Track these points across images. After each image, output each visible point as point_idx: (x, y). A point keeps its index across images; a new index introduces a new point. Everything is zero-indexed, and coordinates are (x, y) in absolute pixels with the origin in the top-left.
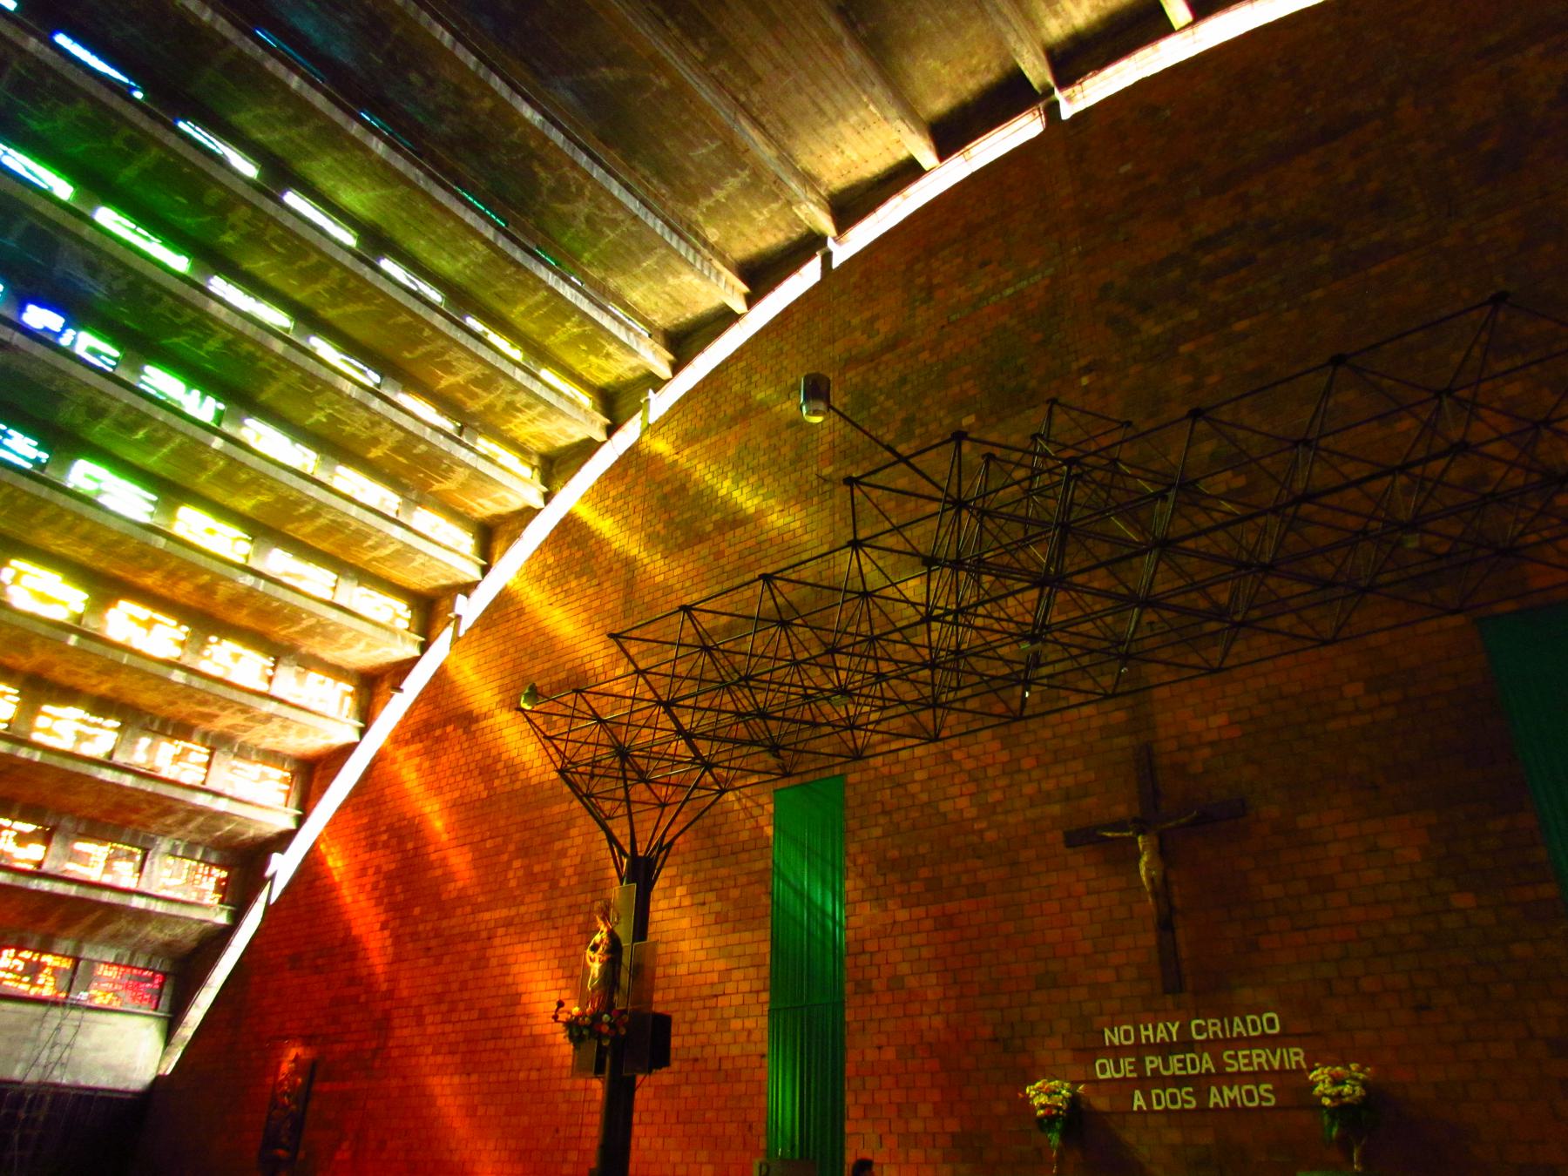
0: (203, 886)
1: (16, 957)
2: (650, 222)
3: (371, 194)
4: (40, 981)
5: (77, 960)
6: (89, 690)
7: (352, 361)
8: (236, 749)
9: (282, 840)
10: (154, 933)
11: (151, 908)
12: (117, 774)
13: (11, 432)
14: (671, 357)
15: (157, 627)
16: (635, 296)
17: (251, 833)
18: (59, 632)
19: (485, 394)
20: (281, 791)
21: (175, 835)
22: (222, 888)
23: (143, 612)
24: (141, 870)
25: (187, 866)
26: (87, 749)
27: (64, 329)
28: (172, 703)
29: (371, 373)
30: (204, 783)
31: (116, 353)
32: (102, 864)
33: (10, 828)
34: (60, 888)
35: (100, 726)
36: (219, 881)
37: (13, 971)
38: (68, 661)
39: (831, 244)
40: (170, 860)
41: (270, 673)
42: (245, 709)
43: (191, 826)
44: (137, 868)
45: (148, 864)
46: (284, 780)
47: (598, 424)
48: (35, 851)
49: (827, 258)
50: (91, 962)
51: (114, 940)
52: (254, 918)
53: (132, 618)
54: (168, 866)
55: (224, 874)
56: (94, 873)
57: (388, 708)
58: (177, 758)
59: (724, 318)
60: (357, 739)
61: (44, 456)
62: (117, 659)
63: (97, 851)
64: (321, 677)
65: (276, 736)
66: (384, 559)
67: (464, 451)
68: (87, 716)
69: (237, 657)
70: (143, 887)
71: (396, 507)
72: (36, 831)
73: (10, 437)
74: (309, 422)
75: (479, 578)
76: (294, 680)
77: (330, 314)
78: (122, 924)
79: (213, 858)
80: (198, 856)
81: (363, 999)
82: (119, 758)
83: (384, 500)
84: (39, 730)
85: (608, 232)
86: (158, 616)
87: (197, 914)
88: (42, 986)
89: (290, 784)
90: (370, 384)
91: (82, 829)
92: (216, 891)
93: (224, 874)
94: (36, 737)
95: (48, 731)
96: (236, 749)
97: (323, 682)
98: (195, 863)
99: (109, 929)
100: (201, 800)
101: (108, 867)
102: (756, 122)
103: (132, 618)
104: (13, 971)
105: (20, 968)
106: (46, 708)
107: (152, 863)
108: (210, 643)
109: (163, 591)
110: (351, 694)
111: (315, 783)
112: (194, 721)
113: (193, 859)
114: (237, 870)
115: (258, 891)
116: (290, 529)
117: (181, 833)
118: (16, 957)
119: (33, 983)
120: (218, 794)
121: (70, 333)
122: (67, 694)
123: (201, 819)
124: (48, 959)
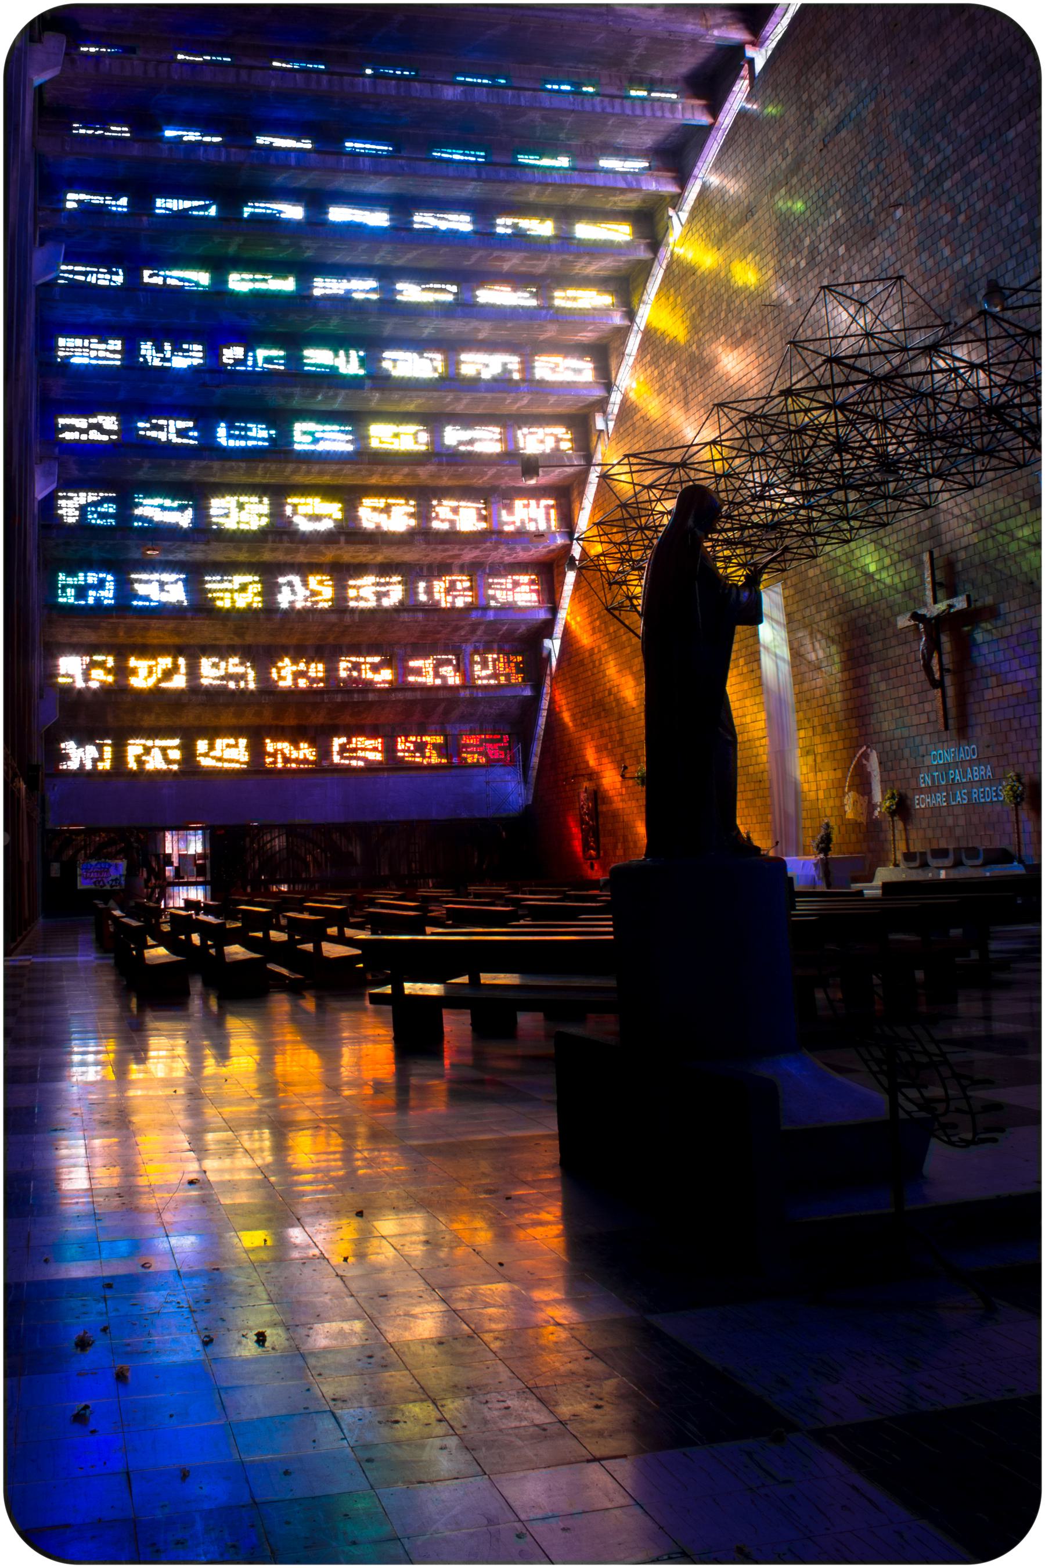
6: (373, 562)
7: (431, 286)
13: (249, 425)
27: (246, 355)
29: (449, 287)
31: (282, 353)
33: (365, 663)
35: (388, 584)
59: (704, 133)
60: (568, 542)
61: (273, 432)
68: (378, 579)
73: (250, 429)
74: (424, 335)
77: (399, 263)
82: (407, 602)
83: (505, 365)
84: (352, 599)
91: (409, 650)
94: (352, 604)
95: (358, 598)
106: (351, 582)
121: (250, 354)
122: (360, 569)
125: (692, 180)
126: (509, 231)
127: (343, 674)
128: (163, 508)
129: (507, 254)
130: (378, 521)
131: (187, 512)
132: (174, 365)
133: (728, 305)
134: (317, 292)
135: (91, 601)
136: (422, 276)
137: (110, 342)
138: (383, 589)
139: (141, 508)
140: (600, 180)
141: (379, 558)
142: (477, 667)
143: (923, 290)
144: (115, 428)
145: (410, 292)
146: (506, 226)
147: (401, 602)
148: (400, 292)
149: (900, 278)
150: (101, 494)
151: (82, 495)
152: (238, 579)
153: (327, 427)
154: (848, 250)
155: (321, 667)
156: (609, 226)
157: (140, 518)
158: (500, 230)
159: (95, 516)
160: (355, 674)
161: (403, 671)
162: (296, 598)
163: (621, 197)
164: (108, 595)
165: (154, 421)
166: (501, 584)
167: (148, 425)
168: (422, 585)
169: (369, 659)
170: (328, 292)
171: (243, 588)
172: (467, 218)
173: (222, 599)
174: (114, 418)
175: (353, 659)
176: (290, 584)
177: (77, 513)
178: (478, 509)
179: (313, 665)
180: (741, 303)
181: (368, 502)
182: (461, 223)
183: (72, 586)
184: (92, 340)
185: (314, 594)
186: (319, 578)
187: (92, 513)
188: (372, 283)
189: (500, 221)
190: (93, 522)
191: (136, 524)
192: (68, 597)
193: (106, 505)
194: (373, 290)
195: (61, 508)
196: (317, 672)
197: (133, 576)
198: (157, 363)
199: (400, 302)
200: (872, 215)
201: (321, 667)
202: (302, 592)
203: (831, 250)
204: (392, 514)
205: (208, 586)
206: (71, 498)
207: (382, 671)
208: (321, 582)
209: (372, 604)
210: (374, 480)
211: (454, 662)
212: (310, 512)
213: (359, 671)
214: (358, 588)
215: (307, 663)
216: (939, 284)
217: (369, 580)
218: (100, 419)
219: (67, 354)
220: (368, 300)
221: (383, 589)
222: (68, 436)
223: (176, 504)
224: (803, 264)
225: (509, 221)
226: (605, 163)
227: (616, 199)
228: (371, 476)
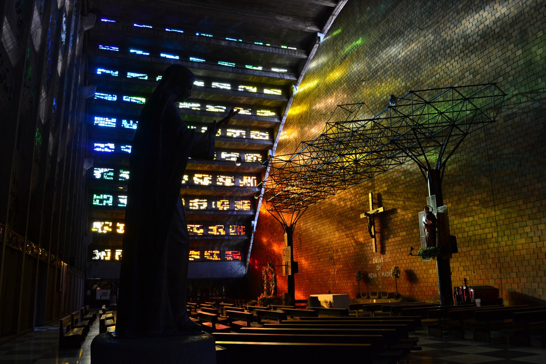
1: (208, 252)
2: (268, 50)
3: (202, 72)
4: (214, 257)
7: (218, 107)
9: (253, 218)
12: (209, 212)
14: (295, 74)
15: (205, 178)
16: (279, 62)
17: (245, 217)
19: (252, 101)
20: (248, 206)
23: (201, 176)
26: (202, 208)
29: (223, 107)
32: (216, 231)
33: (195, 227)
34: (208, 238)
35: (203, 202)
36: (243, 229)
37: (208, 256)
39: (319, 35)
40: (231, 226)
41: (233, 180)
47: (285, 97)
48: (201, 231)
49: (319, 38)
52: (252, 237)
53: (198, 178)
54: (231, 228)
55: (244, 227)
56: (215, 233)
58: (221, 205)
63: (214, 228)
64: (247, 177)
66: (246, 147)
67: (253, 117)
69: (224, 179)
71: (244, 134)
72: (200, 226)
76: (240, 180)
77: (207, 99)
79: (240, 224)
82: (209, 208)
85: (261, 54)
86: (204, 175)
87: (240, 238)
88: (215, 258)
90: (223, 111)
94: (191, 208)
95: (193, 206)
97: (248, 179)
100: (230, 213)
101: (218, 231)
102: (282, 14)
103: (198, 178)
104: (208, 256)
105: (209, 255)
106: (191, 201)
108: (218, 178)
112: (222, 195)
116: (223, 147)
117: (230, 220)
119: (213, 257)
122: (194, 197)
124: (214, 252)
125: (300, 77)
126: (243, 90)
129: (242, 98)
132: (133, 128)
133: (310, 115)
134: (180, 107)
135: (104, 204)
136: (214, 104)
137: (112, 119)
140: (271, 75)
141: (200, 194)
142: (231, 229)
143: (371, 108)
144: (114, 148)
145: (211, 108)
146: (241, 88)
147: (207, 208)
148: (208, 108)
149: (363, 103)
150: (109, 169)
151: (102, 169)
154: (347, 96)
156: (274, 90)
157: (122, 178)
158: (240, 90)
159: (106, 176)
160: (191, 230)
161: (206, 229)
163: (279, 81)
164: (110, 202)
165: (127, 146)
167: (125, 147)
168: (213, 203)
169: (196, 226)
170: (184, 107)
172: (229, 85)
174: (113, 144)
177: (101, 175)
180: (314, 114)
181: (197, 175)
182: (227, 86)
183: (98, 199)
184: (106, 118)
187: (105, 175)
188: (199, 105)
189: (240, 87)
190: (106, 178)
191: (120, 179)
192: (96, 203)
193: (110, 173)
194: (199, 107)
195: (95, 173)
197: (119, 196)
198: (128, 127)
199: (208, 111)
200: (355, 85)
203: (342, 96)
204: (204, 179)
206: (99, 170)
207: (200, 230)
209: (197, 208)
210: (199, 168)
211: (223, 228)
213: (193, 230)
214: (193, 203)
216: (376, 106)
217: (197, 200)
218: (109, 145)
219: (98, 122)
220: (196, 110)
222: (98, 149)
224: (333, 101)
225: (243, 87)
226: (273, 70)
227: (277, 81)
228: (197, 167)
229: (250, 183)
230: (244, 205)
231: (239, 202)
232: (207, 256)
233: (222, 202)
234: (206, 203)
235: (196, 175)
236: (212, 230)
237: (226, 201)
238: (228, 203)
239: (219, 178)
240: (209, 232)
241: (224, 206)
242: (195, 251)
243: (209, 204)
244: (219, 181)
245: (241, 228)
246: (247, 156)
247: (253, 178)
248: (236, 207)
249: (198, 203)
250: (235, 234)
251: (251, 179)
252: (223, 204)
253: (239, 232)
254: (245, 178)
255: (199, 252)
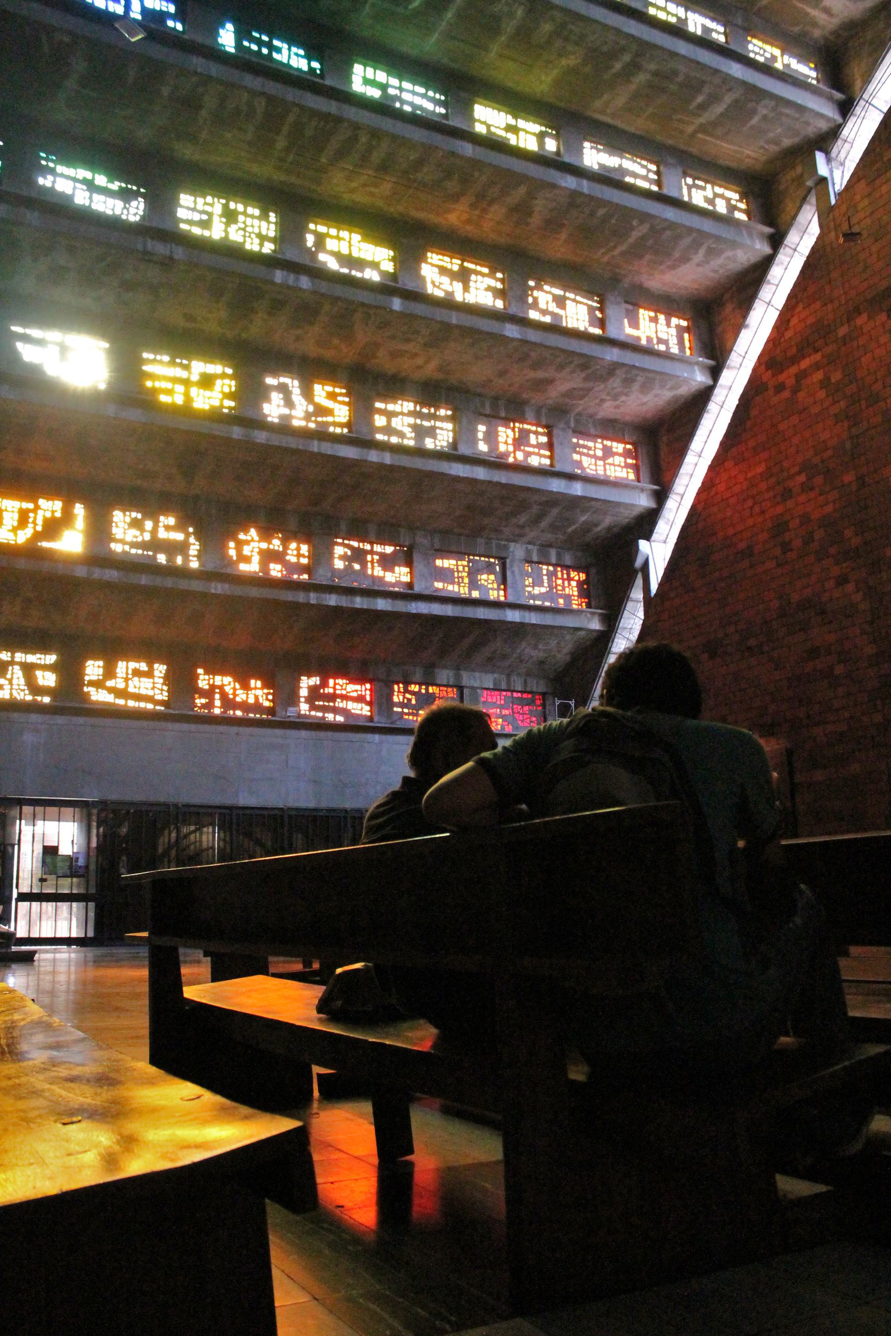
0: (567, 591)
1: (406, 691)
5: (461, 689)
8: (572, 424)
10: (531, 651)
11: (527, 621)
12: (468, 467)
18: (380, 297)
20: (627, 466)
21: (526, 539)
22: (585, 591)
24: (504, 581)
25: (545, 572)
28: (502, 373)
30: (552, 465)
32: (466, 580)
33: (372, 552)
34: (437, 609)
35: (434, 417)
36: (580, 584)
38: (393, 337)
42: (586, 363)
43: (544, 524)
44: (500, 580)
45: (509, 573)
46: (626, 454)
48: (400, 575)
50: (473, 688)
51: (490, 664)
57: (745, 336)
62: (446, 319)
64: (652, 314)
65: (615, 398)
69: (560, 302)
70: (511, 599)
73: (279, 50)
75: (840, 120)
78: (498, 645)
80: (554, 561)
81: (839, 670)
82: (463, 450)
86: (468, 265)
89: (636, 458)
92: (580, 596)
93: (583, 576)
94: (379, 437)
95: (388, 430)
96: (572, 424)
98: (551, 568)
99: (486, 651)
100: (556, 486)
101: (474, 584)
103: (443, 270)
105: (413, 702)
106: (379, 405)
107: (513, 572)
109: (470, 230)
110: (688, 329)
111: (664, 450)
113: (548, 564)
114: (593, 570)
115: (628, 586)
117: (532, 534)
118: (406, 691)
120: (571, 477)
123: (555, 511)
127: (339, 564)
128: (91, 186)
130: (450, 289)
131: (134, 203)
138: (426, 424)
139: (50, 178)
152: (199, 367)
153: (407, 85)
155: (304, 549)
160: (357, 567)
162: (294, 413)
166: (589, 448)
169: (378, 548)
171: (207, 381)
173: (169, 392)
175: (355, 544)
176: (283, 389)
178: (591, 310)
179: (293, 545)
185: (321, 411)
186: (329, 389)
196: (299, 555)
201: (304, 549)
202: (301, 406)
205: (146, 368)
208: (332, 396)
212: (345, 251)
213: (364, 564)
214: (390, 415)
215: (285, 542)
221: (426, 424)
223: (115, 186)
229: (666, 342)
230: (610, 460)
231: (591, 444)
232: (402, 705)
233: (521, 431)
234: (450, 426)
235: (434, 258)
236: (446, 575)
237: (534, 428)
238: (544, 439)
239: (536, 293)
240: (439, 585)
241: (528, 449)
242: (353, 681)
243: (463, 433)
244: (535, 305)
245: (570, 579)
246: (690, 188)
247: (674, 321)
248: (579, 464)
249: (411, 420)
250: (547, 604)
251: (668, 325)
252: (520, 441)
253: (561, 596)
254: (644, 315)
255: (368, 686)
